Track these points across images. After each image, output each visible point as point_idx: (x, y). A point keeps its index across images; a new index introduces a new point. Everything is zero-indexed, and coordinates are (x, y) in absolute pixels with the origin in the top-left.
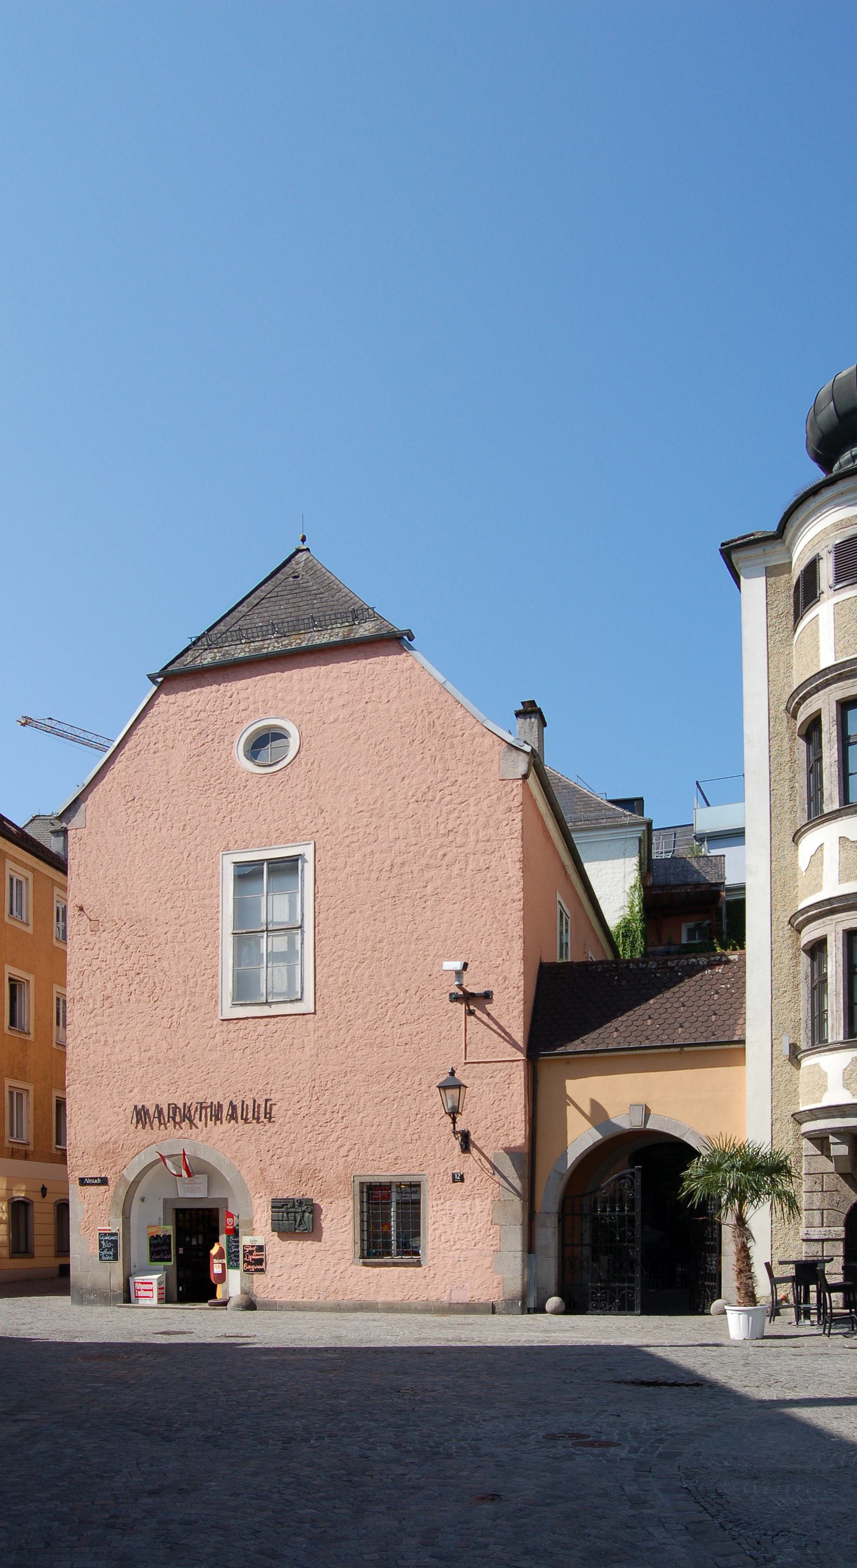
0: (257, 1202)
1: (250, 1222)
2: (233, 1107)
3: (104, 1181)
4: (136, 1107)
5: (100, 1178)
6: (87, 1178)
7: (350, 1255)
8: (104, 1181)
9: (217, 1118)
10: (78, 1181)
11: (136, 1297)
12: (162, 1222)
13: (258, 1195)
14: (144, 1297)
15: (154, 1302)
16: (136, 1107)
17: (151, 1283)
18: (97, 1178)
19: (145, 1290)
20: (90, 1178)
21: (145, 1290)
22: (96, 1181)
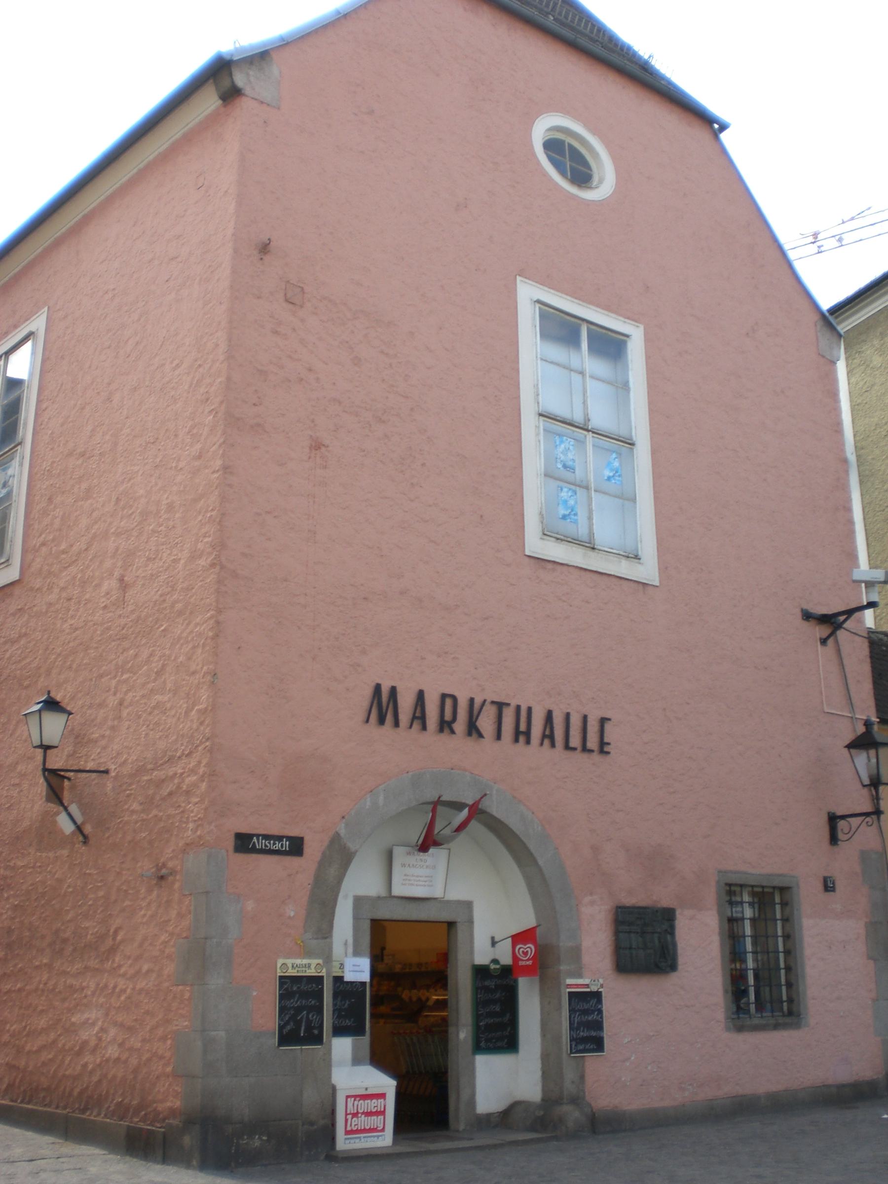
0: (586, 911)
1: (576, 953)
2: (549, 717)
3: (296, 847)
4: (378, 688)
5: (289, 838)
6: (258, 836)
7: (720, 1014)
8: (296, 847)
9: (522, 735)
10: (230, 843)
11: (347, 1132)
12: (350, 950)
13: (587, 899)
14: (364, 1131)
15: (385, 1140)
16: (378, 688)
17: (382, 1096)
18: (280, 838)
19: (368, 1114)
20: (267, 837)
21: (368, 1114)
22: (278, 846)
